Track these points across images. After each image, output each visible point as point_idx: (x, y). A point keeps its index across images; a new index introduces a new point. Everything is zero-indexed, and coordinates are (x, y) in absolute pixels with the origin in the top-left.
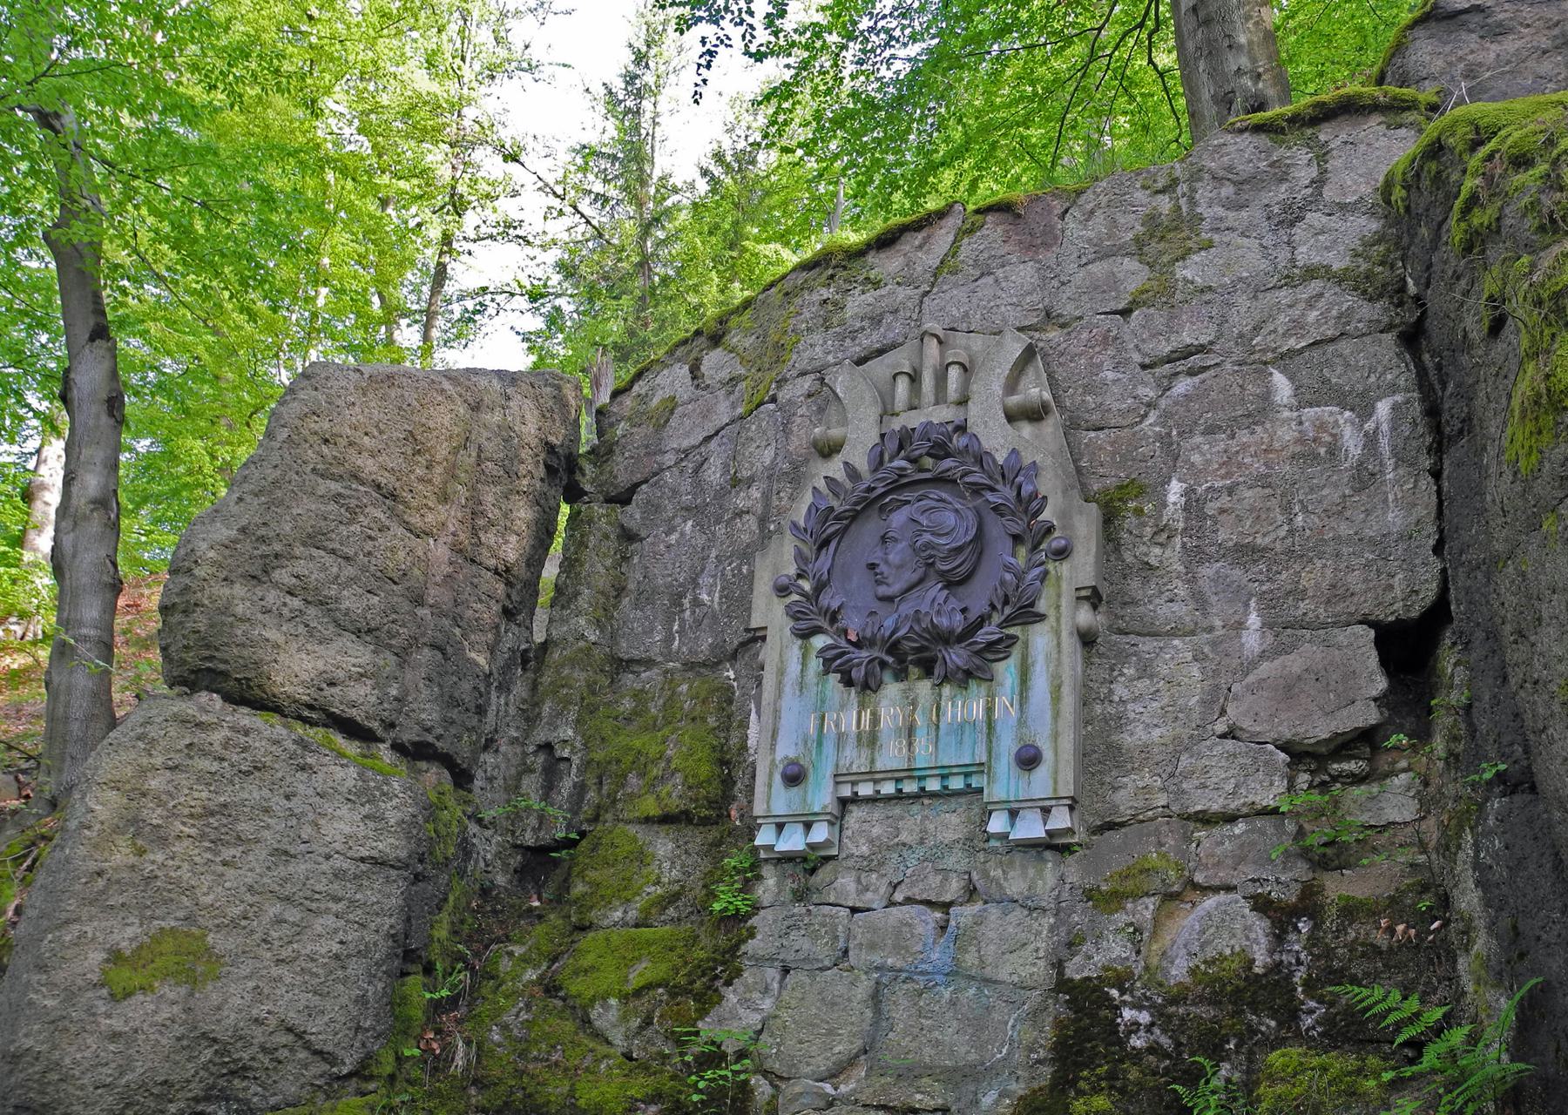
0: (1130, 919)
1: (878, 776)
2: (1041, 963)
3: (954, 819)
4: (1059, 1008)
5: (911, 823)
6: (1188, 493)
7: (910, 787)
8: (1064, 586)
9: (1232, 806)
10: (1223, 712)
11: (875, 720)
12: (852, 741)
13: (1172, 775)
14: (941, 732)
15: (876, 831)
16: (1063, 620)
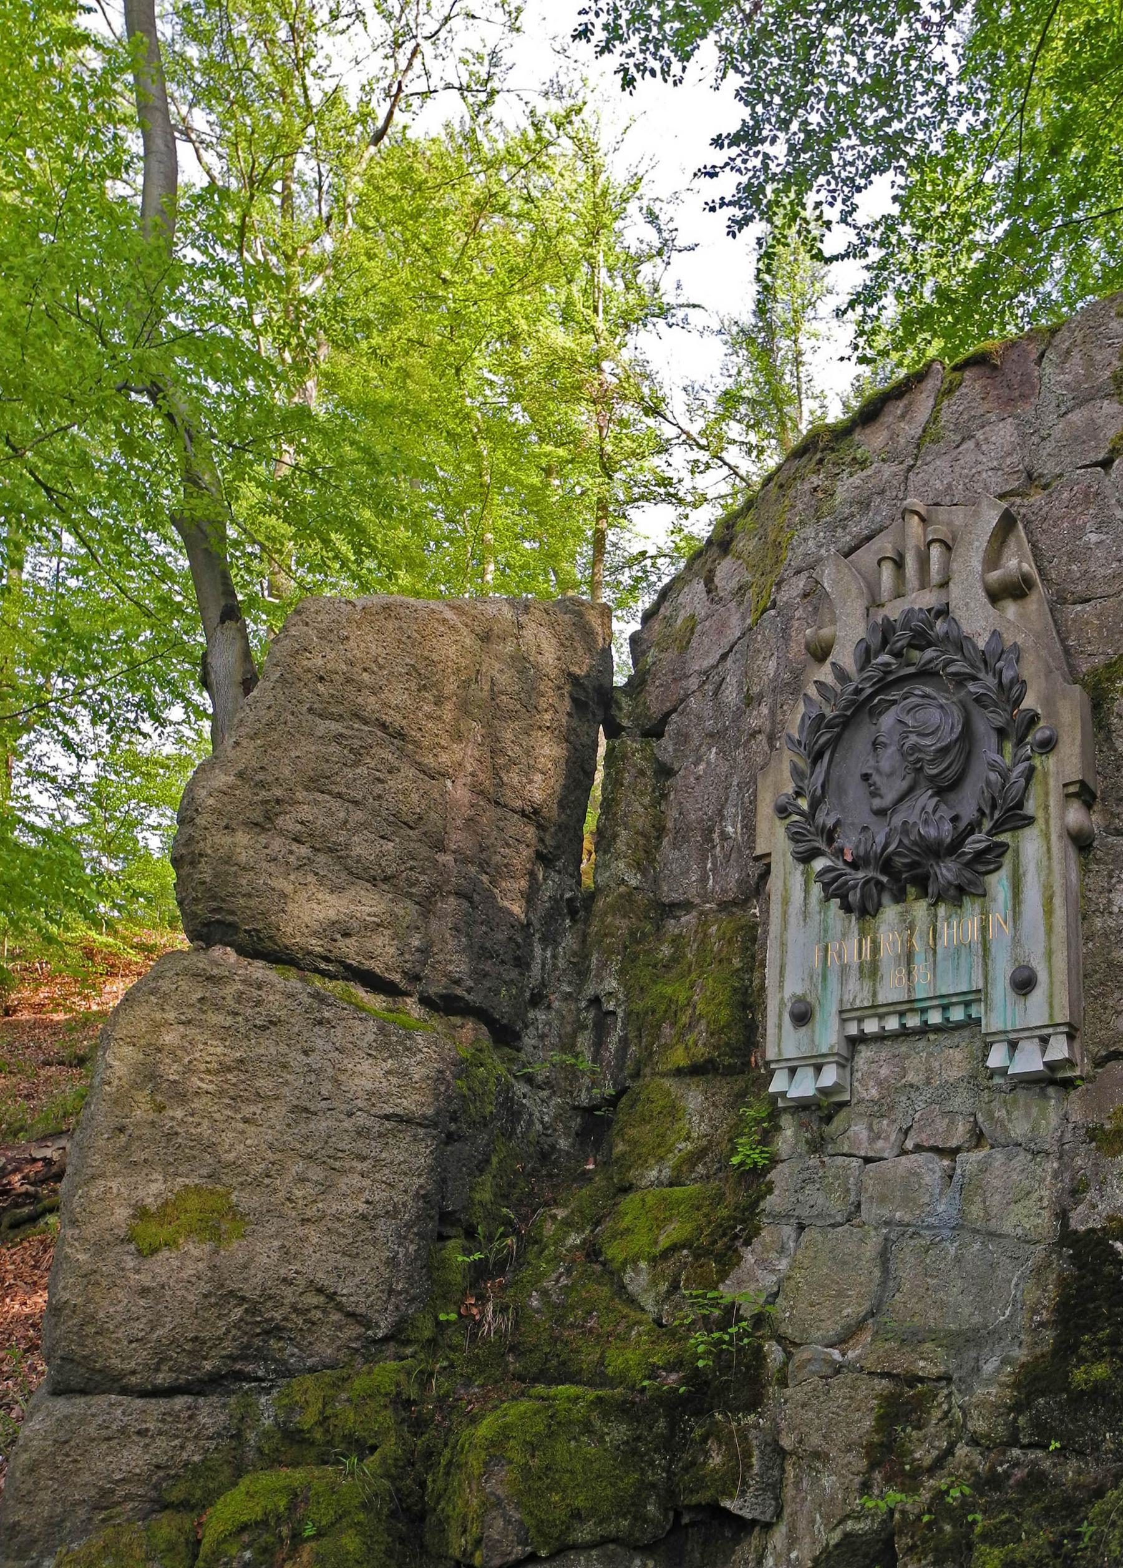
1: (881, 1010)
2: (1045, 1213)
3: (957, 1055)
4: (1062, 1265)
5: (918, 1060)
7: (913, 1021)
8: (1052, 782)
11: (876, 949)
12: (854, 973)
14: (939, 957)
15: (884, 1072)
16: (1052, 822)
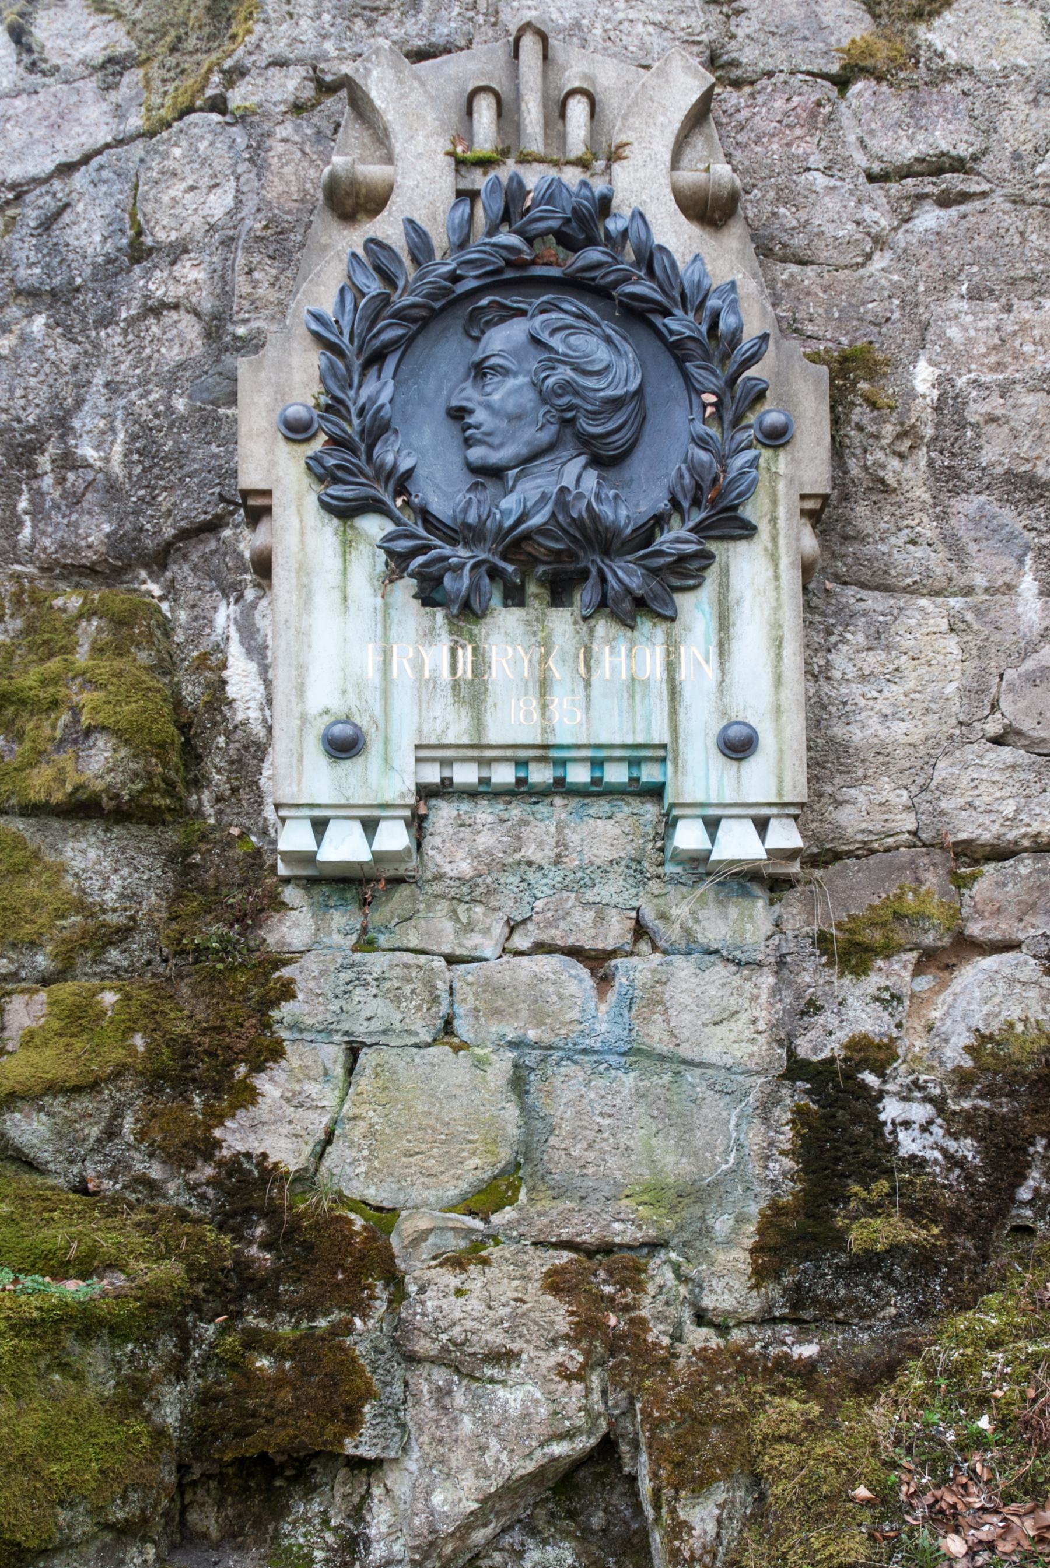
0: (883, 982)
2: (762, 1039)
3: (610, 829)
6: (942, 382)
7: (540, 775)
9: (1011, 836)
10: (995, 707)
13: (924, 789)
14: (595, 693)
15: (485, 840)
16: (782, 541)
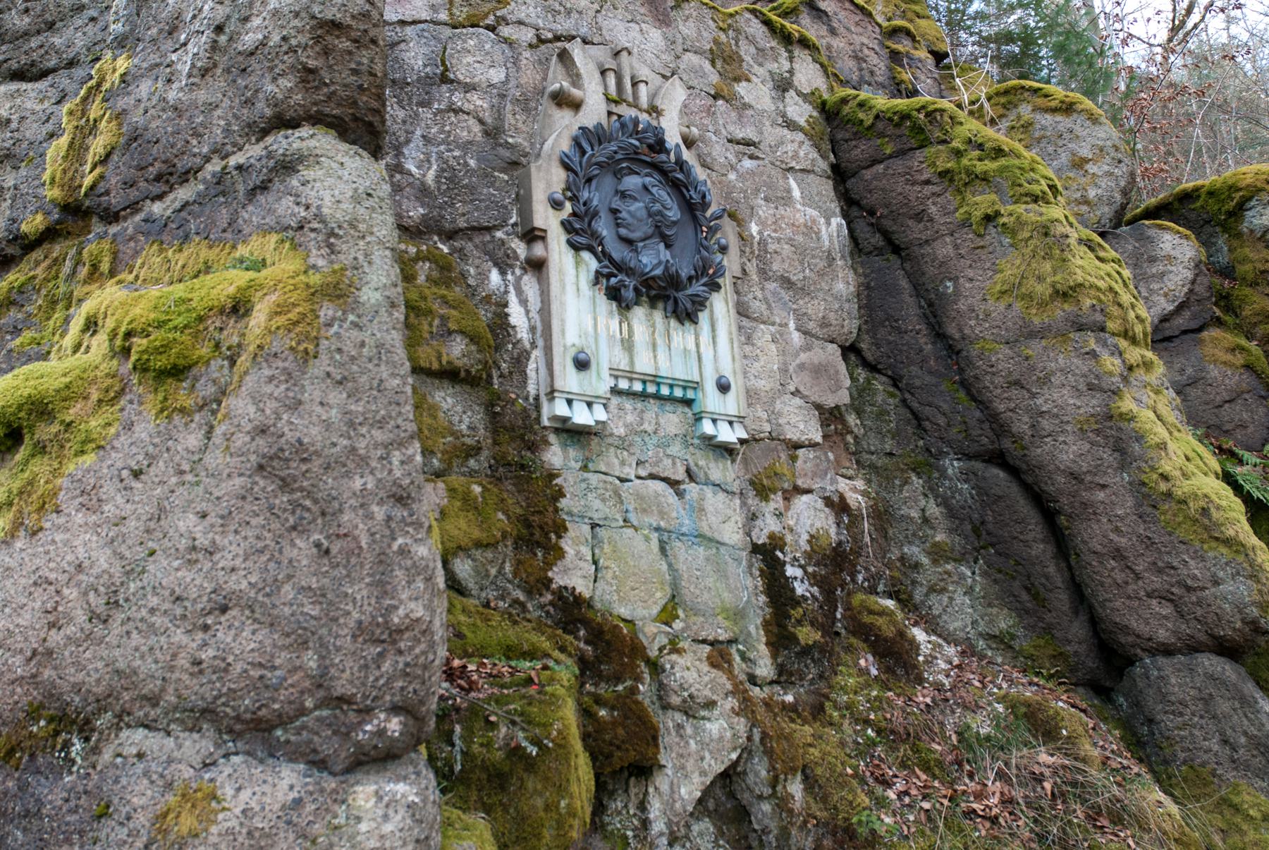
7: (651, 389)
15: (630, 418)
